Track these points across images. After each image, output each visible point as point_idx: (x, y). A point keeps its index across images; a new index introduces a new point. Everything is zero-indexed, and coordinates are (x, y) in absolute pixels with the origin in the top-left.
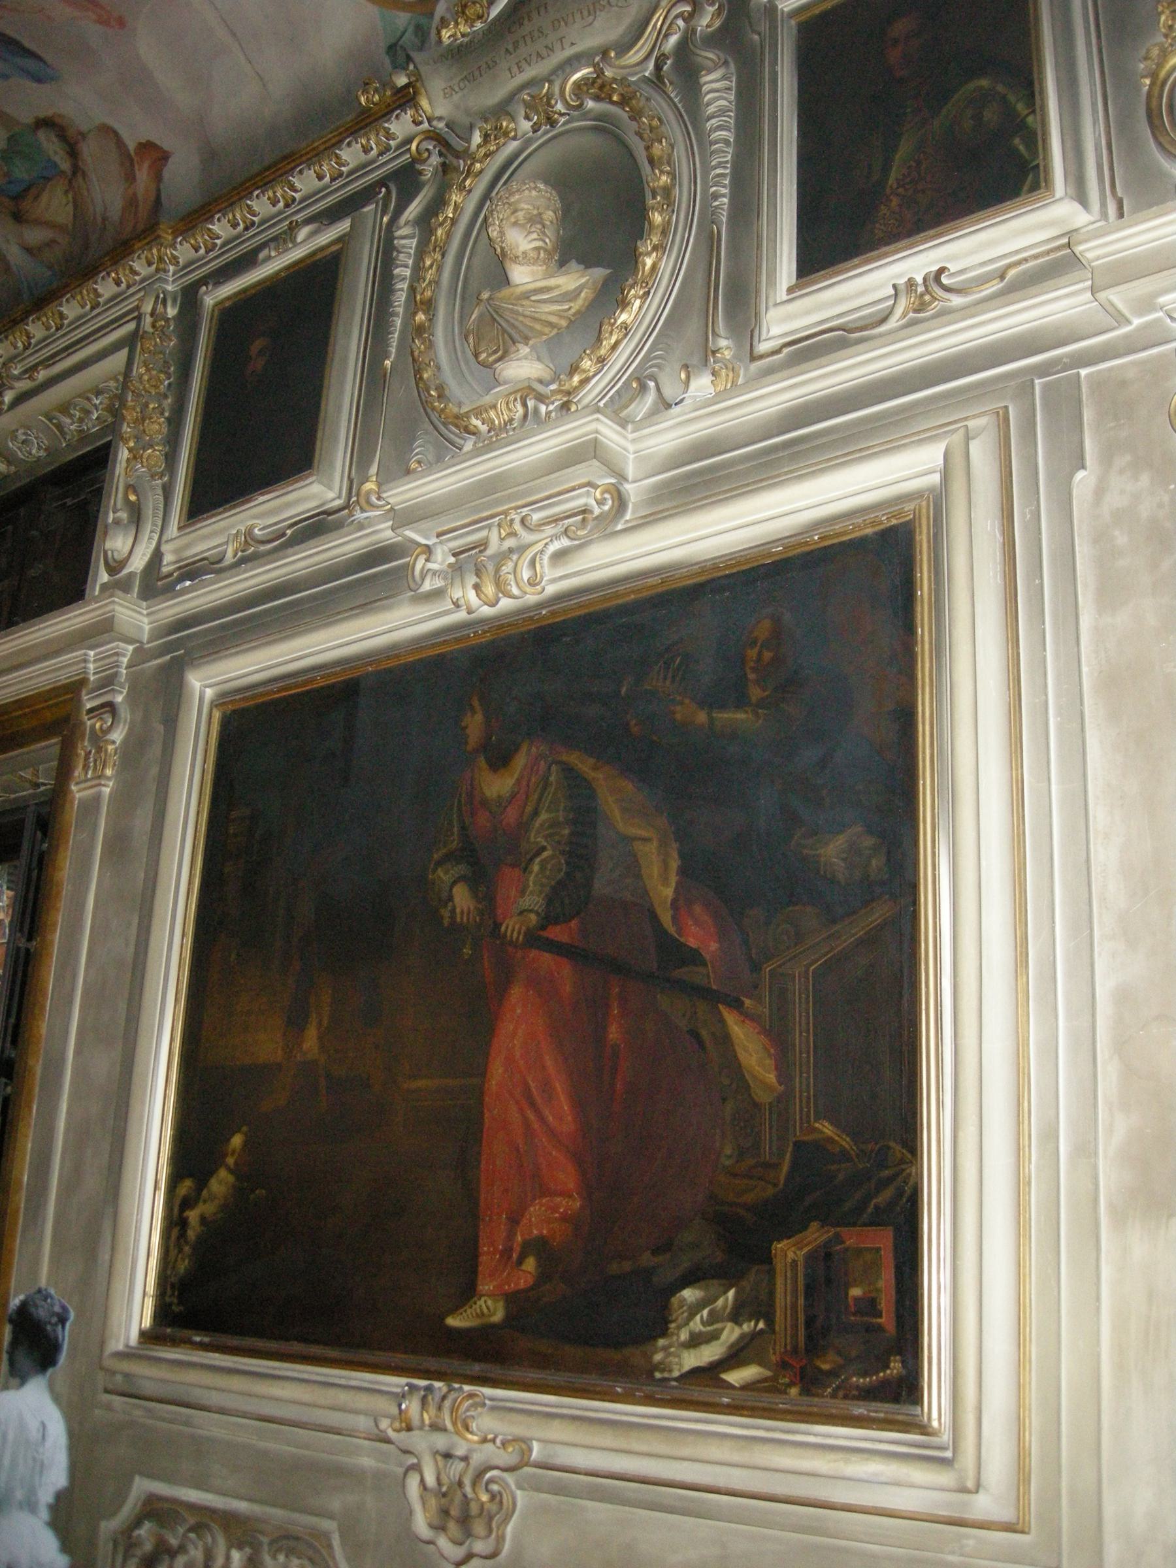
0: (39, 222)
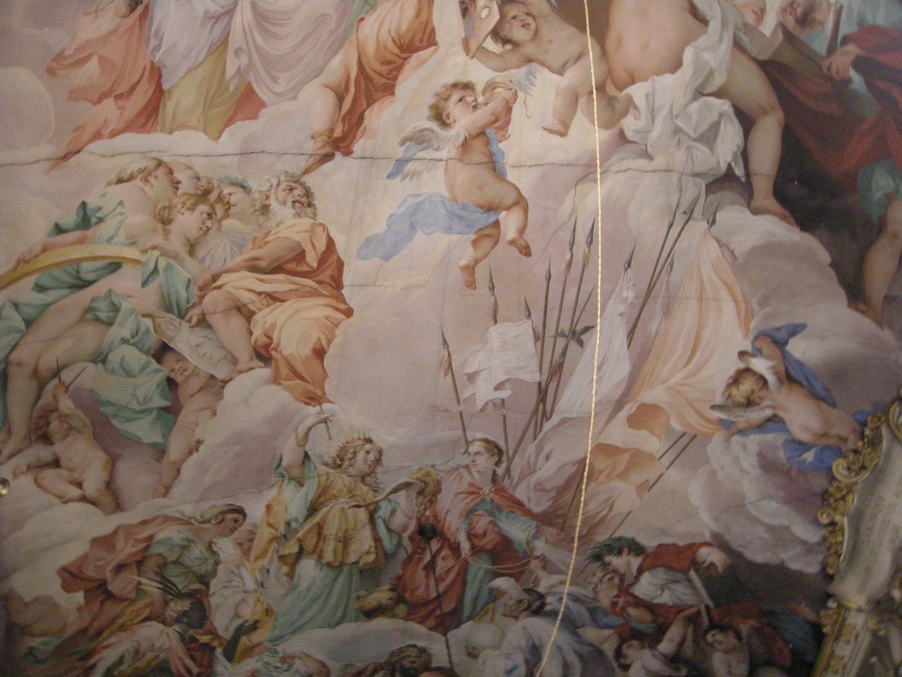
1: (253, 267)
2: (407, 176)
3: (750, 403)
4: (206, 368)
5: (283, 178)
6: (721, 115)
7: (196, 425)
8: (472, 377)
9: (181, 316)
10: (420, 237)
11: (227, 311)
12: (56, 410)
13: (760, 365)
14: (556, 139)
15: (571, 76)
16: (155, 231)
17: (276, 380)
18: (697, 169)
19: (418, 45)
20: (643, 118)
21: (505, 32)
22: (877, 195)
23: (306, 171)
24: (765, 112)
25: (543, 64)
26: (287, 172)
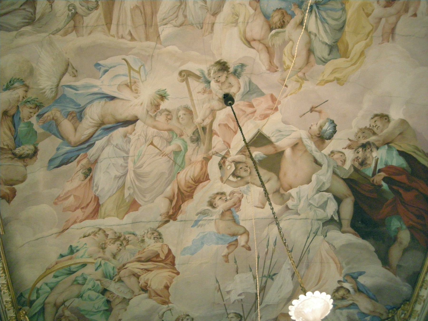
1: (139, 260)
2: (199, 226)
3: (343, 298)
4: (122, 295)
5: (149, 230)
6: (328, 198)
7: (119, 314)
8: (228, 292)
9: (111, 279)
10: (205, 246)
11: (129, 276)
12: (64, 315)
13: (347, 285)
14: (260, 210)
16: (99, 252)
17: (150, 297)
18: (319, 218)
19: (202, 180)
20: (296, 200)
21: (238, 173)
22: (393, 228)
23: (159, 227)
24: (347, 197)
26: (151, 228)
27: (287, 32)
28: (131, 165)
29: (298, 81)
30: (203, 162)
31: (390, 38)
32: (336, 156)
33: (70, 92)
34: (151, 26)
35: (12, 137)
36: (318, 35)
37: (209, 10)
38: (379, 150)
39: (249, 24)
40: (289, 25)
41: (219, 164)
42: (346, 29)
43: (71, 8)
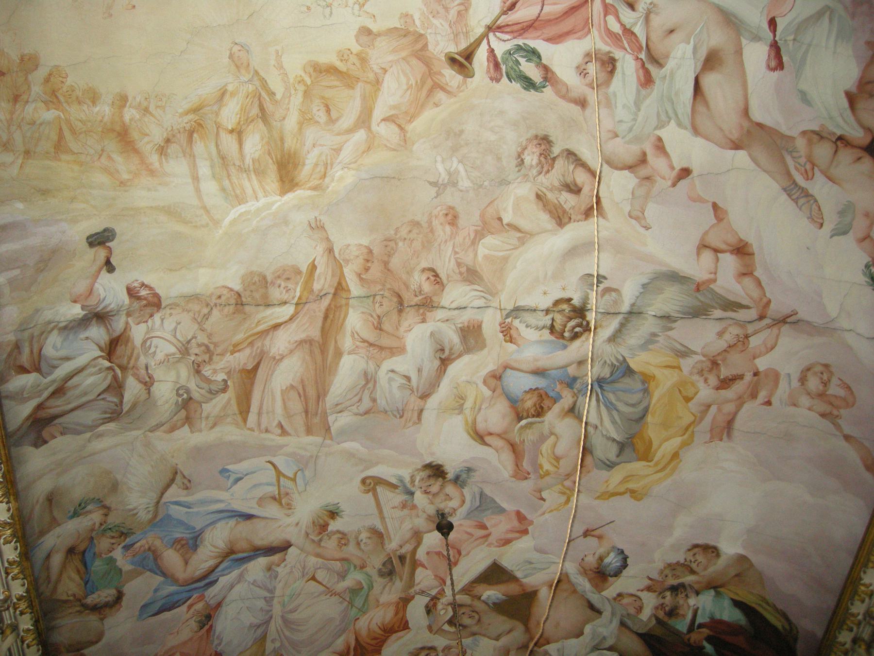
0: (64, 566)
15: (503, 641)
25: (484, 635)
27: (546, 423)
28: (277, 610)
29: (564, 493)
30: (398, 603)
31: (725, 435)
32: (625, 601)
33: (177, 512)
34: (317, 414)
35: (81, 582)
36: (600, 427)
37: (415, 390)
38: (700, 596)
39: (482, 412)
40: (550, 413)
41: (427, 606)
42: (649, 418)
43: (181, 392)
